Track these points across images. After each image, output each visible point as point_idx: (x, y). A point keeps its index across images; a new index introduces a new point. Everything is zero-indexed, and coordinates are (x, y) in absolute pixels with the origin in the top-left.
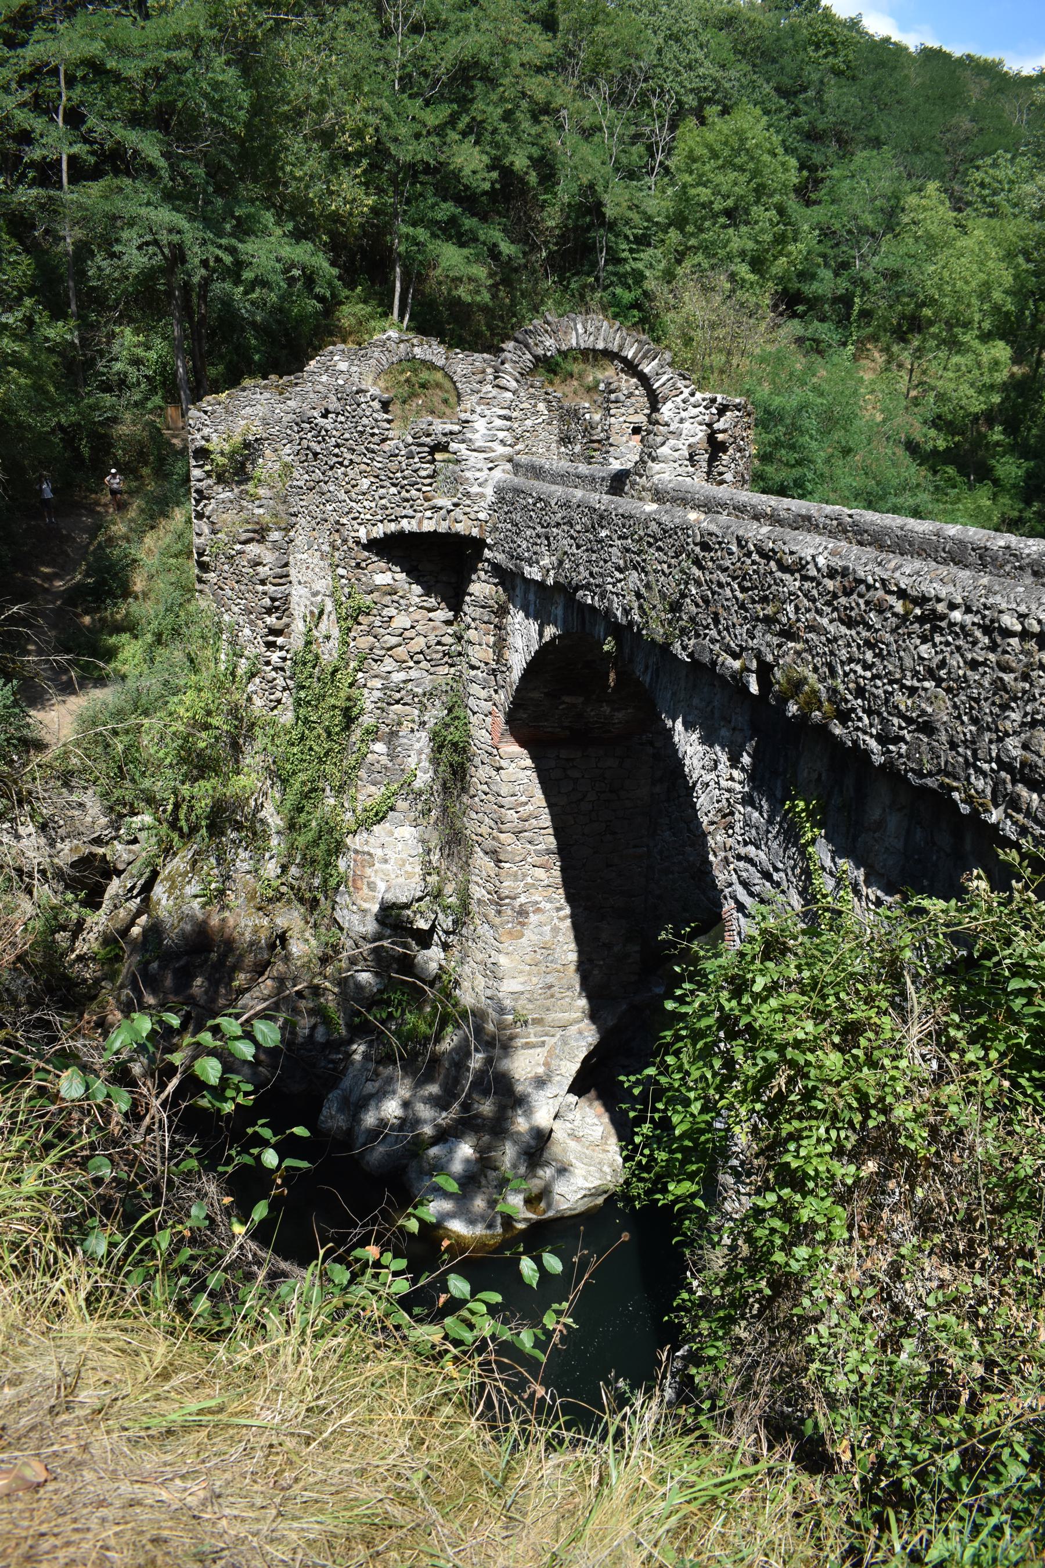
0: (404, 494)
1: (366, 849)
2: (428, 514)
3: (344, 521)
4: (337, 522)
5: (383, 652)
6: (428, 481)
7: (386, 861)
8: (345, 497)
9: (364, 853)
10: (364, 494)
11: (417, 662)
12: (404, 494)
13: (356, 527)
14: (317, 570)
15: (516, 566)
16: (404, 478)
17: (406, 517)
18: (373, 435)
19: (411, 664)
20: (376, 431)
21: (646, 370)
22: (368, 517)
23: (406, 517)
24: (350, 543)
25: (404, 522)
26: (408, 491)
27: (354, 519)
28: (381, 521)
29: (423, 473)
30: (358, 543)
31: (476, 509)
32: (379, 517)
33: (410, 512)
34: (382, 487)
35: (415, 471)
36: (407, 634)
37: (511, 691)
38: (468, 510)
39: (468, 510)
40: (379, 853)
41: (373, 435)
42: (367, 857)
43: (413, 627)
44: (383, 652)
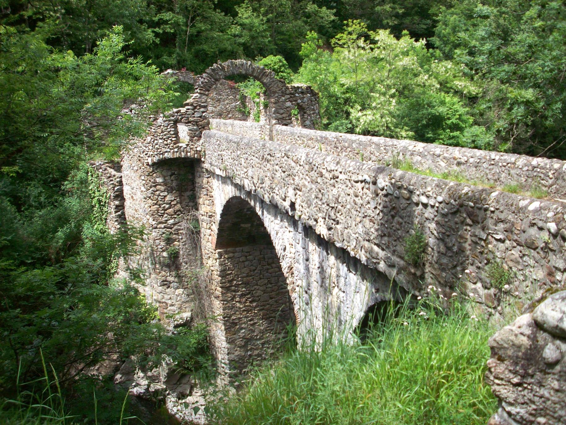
0: (165, 142)
1: (163, 300)
2: (176, 150)
3: (142, 156)
4: (139, 156)
5: (163, 212)
6: (174, 136)
7: (173, 305)
8: (140, 144)
9: (163, 302)
10: (149, 143)
11: (178, 215)
12: (165, 142)
13: (147, 158)
14: (133, 178)
15: (213, 169)
16: (165, 135)
17: (166, 152)
18: (150, 118)
19: (175, 216)
20: (152, 116)
21: (265, 81)
22: (152, 153)
23: (166, 152)
24: (145, 164)
25: (166, 154)
26: (167, 141)
27: (146, 154)
28: (157, 155)
29: (172, 133)
30: (148, 164)
31: (196, 146)
32: (156, 153)
33: (169, 150)
34: (157, 140)
35: (169, 132)
36: (172, 203)
37: (217, 223)
38: (192, 147)
39: (192, 147)
40: (169, 302)
41: (150, 118)
42: (164, 304)
43: (175, 200)
44: (163, 212)
